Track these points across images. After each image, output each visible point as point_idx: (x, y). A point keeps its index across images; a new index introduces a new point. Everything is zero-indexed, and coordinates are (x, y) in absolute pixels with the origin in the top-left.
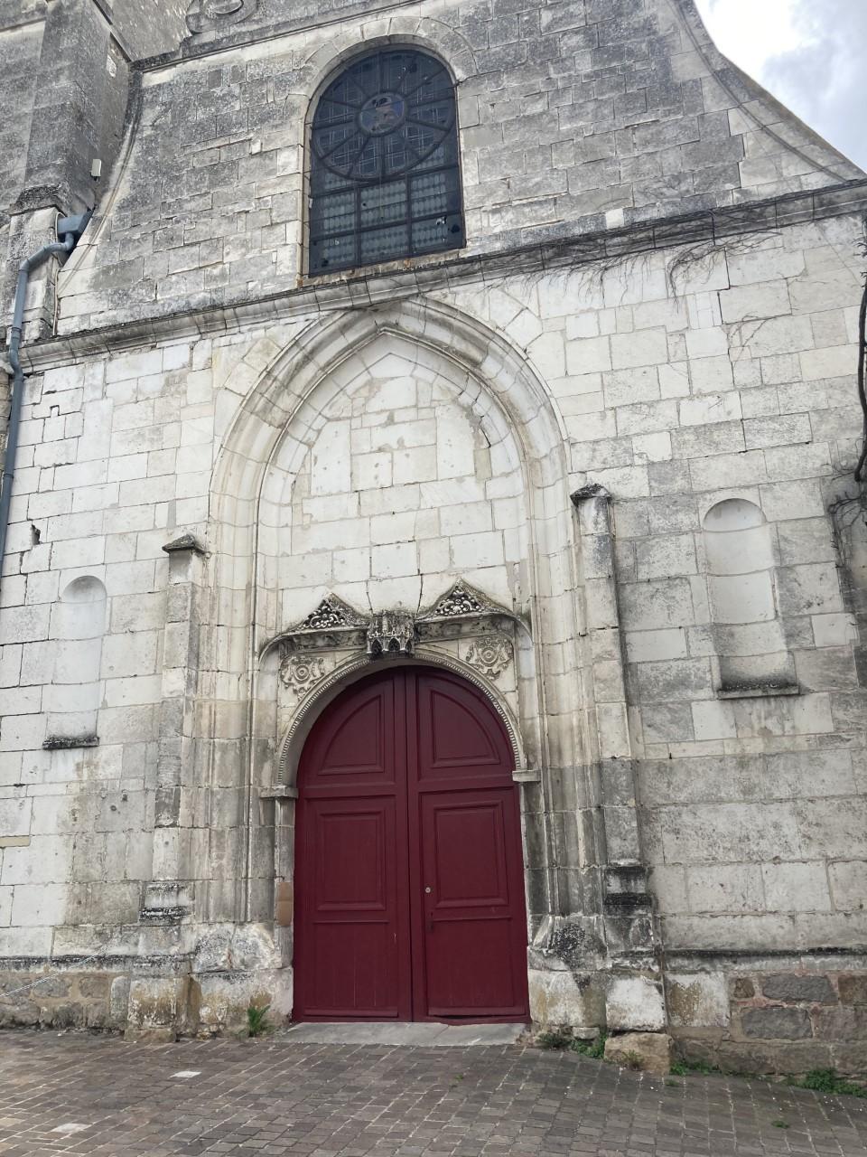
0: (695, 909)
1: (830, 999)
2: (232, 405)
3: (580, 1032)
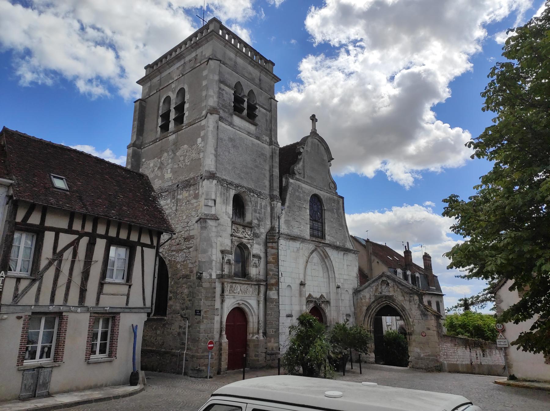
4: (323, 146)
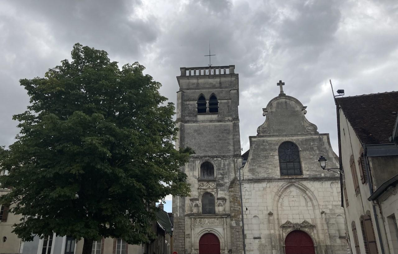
2: (274, 194)
4: (293, 101)
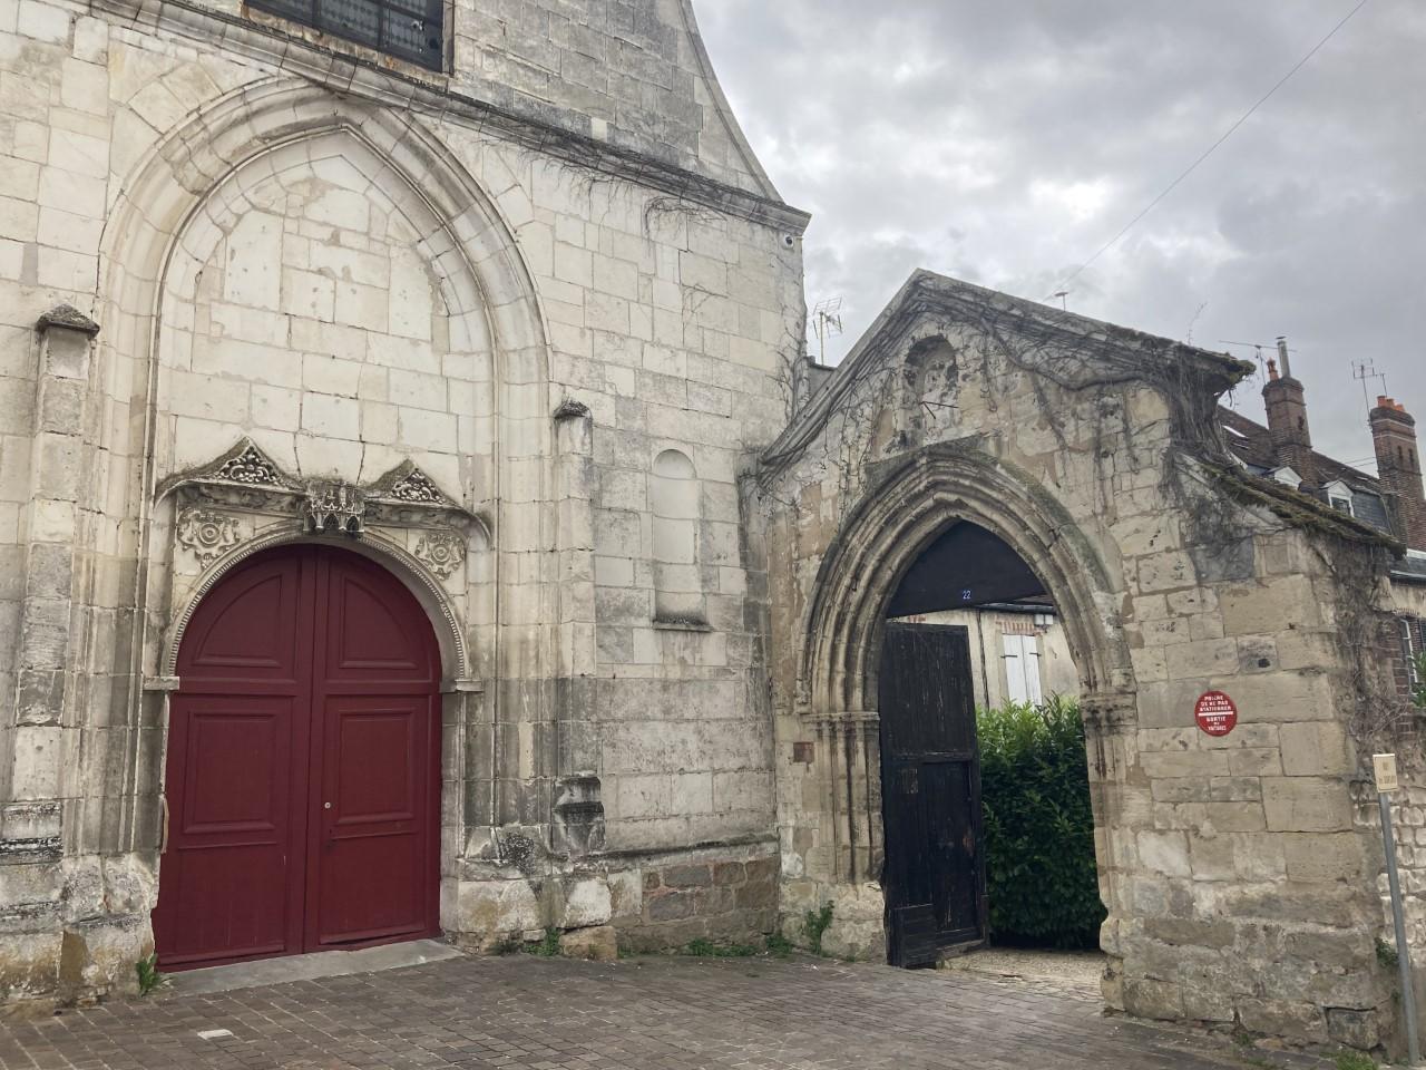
0: (623, 815)
1: (707, 884)
3: (537, 935)
